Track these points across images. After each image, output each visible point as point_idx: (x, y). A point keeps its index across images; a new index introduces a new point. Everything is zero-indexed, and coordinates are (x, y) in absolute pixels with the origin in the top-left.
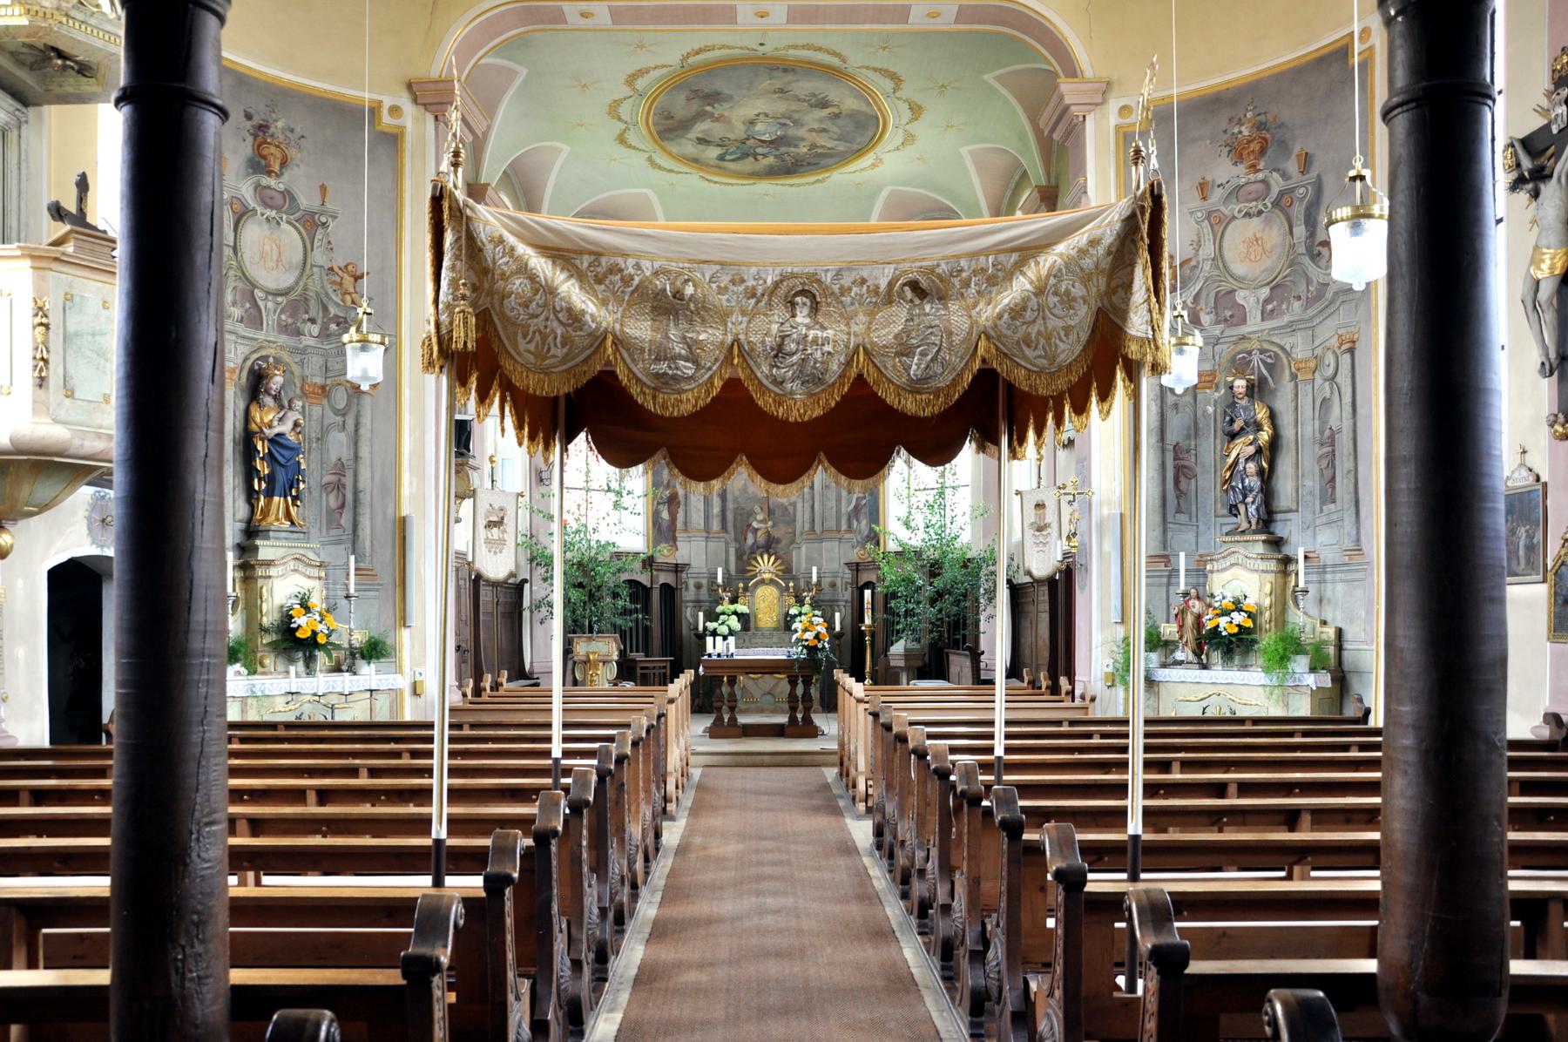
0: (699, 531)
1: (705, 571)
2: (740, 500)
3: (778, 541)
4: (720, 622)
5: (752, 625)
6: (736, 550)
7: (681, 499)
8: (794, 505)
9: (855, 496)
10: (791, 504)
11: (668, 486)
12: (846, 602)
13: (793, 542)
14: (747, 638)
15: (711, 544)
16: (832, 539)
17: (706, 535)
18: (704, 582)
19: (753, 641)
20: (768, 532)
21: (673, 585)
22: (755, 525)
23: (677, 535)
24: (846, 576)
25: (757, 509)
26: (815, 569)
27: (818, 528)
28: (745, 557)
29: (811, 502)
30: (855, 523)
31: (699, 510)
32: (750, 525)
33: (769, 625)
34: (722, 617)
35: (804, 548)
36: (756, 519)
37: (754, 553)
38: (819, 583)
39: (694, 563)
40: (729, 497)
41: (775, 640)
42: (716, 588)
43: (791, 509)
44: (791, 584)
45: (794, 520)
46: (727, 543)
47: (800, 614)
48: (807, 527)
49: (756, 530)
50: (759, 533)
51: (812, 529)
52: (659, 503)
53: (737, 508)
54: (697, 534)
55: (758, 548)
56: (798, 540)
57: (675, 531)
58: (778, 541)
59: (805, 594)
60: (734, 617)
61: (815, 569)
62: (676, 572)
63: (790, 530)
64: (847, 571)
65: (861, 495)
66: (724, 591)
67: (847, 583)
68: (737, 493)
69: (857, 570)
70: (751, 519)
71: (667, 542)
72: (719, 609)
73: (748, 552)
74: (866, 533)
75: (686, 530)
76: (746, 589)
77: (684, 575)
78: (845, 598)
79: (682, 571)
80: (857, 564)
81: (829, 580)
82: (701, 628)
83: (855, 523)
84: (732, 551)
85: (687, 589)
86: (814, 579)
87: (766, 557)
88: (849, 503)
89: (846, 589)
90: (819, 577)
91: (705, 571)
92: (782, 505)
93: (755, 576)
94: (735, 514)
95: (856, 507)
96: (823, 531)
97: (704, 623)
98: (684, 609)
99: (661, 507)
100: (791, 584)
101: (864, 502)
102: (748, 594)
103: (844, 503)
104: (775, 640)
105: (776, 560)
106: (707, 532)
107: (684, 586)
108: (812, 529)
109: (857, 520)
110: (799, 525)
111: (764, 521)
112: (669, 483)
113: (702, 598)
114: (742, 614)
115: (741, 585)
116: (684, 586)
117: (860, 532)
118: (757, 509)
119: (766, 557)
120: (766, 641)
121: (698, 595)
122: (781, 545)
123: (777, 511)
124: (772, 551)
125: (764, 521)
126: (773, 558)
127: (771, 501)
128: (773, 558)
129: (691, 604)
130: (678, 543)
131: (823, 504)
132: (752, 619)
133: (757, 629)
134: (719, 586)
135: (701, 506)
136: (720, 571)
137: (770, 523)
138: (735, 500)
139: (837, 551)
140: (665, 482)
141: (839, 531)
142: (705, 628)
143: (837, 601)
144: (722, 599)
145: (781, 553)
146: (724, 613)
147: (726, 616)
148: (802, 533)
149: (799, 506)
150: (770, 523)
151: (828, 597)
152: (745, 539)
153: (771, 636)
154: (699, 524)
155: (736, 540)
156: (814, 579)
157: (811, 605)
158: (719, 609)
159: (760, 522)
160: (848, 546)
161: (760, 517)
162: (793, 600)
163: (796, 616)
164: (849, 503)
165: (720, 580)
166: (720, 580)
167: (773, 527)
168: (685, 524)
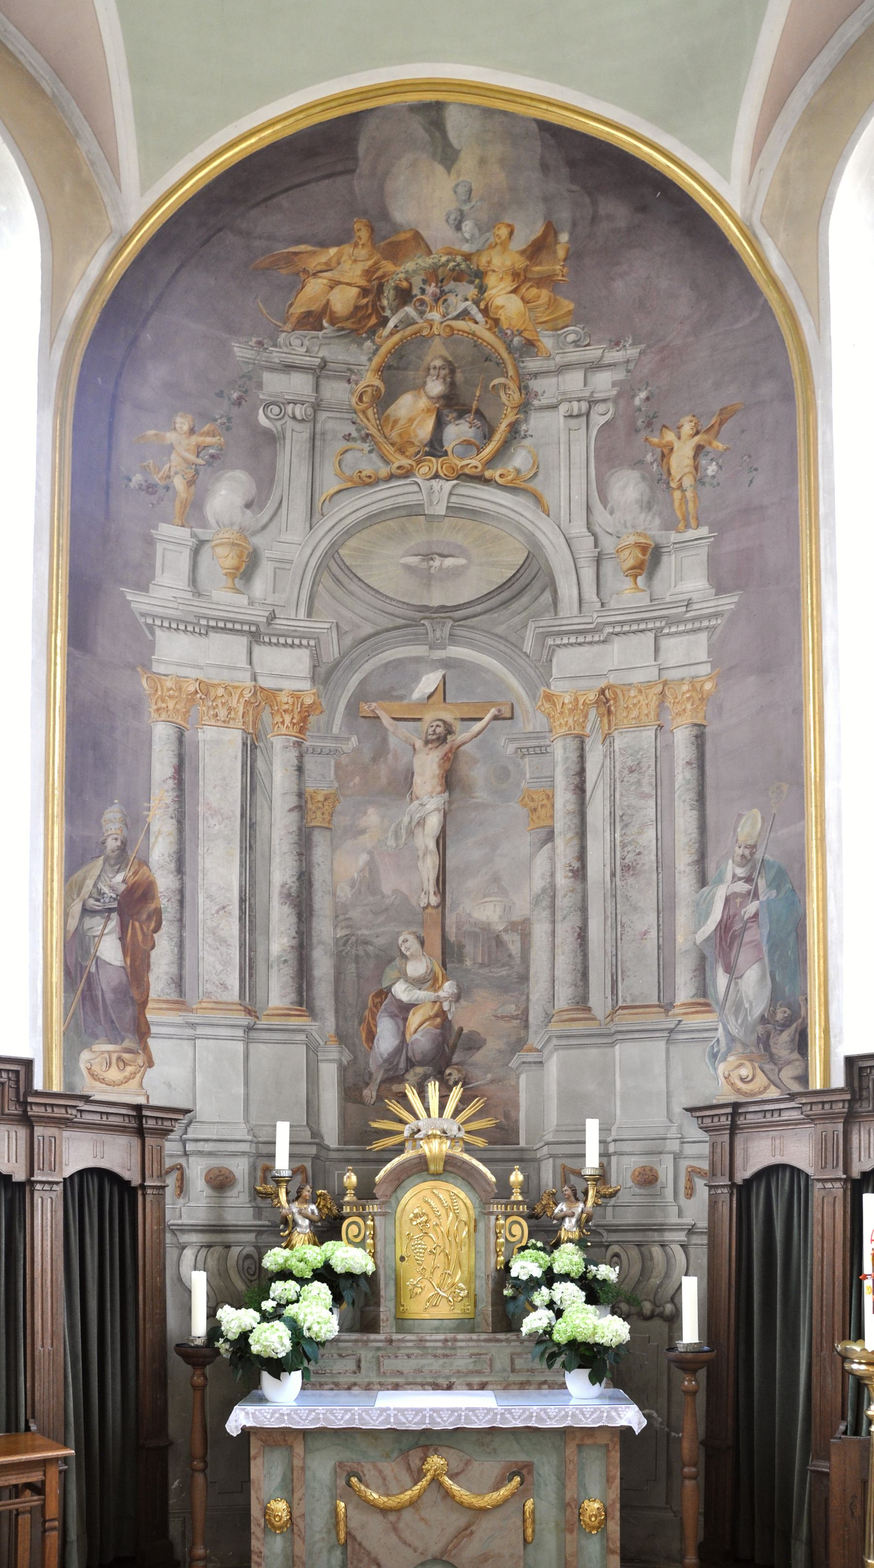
0: (220, 1005)
1: (241, 1132)
2: (355, 914)
3: (474, 1043)
4: (268, 1305)
5: (386, 1310)
6: (343, 1070)
7: (165, 901)
8: (523, 928)
9: (721, 893)
10: (513, 926)
11: (121, 857)
12: (691, 1231)
13: (519, 1044)
14: (366, 1355)
15: (260, 1051)
16: (646, 1033)
17: (245, 1020)
18: (240, 1168)
19: (389, 1364)
20: (442, 1014)
21: (132, 1176)
22: (401, 991)
23: (150, 1016)
24: (689, 1149)
25: (409, 943)
26: (592, 1127)
27: (599, 1000)
28: (370, 1093)
29: (574, 920)
30: (722, 979)
31: (224, 941)
32: (384, 993)
33: (444, 1311)
34: (279, 1289)
35: (553, 1065)
36: (403, 975)
37: (400, 1079)
38: (602, 1177)
39: (204, 1109)
40: (322, 903)
41: (462, 1362)
42: (270, 1187)
43: (513, 943)
44: (517, 1177)
45: (524, 978)
46: (312, 1049)
47: (550, 1278)
48: (564, 996)
49: (404, 1009)
50: (414, 1019)
51: (582, 1002)
52: (86, 911)
53: (346, 939)
54: (217, 1016)
55: (411, 1064)
56: (535, 1040)
57: (143, 1004)
58: (474, 1043)
59: (562, 1207)
60: (321, 1291)
61: (592, 1127)
62: (140, 1132)
63: (511, 1009)
64: (694, 1132)
65: (742, 887)
66: (296, 1197)
67: (693, 1172)
68: (345, 893)
69: (733, 1129)
70: (390, 973)
71: (115, 1037)
72: (274, 1258)
73: (379, 1076)
74: (759, 1009)
75: (180, 1003)
76: (366, 1192)
77: (171, 1146)
78: (688, 1220)
79: (165, 1133)
80: (736, 1106)
81: (632, 1163)
82: (199, 1328)
83: (722, 979)
84: (329, 1074)
85: (182, 1188)
86: (592, 1162)
87: (433, 1090)
88: (701, 915)
89: (690, 1192)
90: (604, 1155)
91: (241, 1132)
92: (486, 928)
93: (399, 1149)
94: (340, 960)
95: (725, 927)
96: (614, 1011)
97: (211, 1314)
98: (171, 1254)
99: (95, 924)
100: (517, 1177)
101: (752, 908)
102: (373, 1208)
103: (683, 917)
104: (462, 1362)
105: (464, 1101)
106: (249, 1012)
107: (171, 1181)
108: (582, 1002)
109: (729, 969)
110: (538, 990)
111: (429, 981)
112: (123, 848)
113: (231, 1218)
114: (350, 1276)
115: (351, 1179)
116: (171, 1181)
117: (738, 1007)
118: (409, 943)
119: (433, 1090)
120: (436, 1365)
121: (218, 1208)
122: (479, 1057)
123: (469, 949)
124: (453, 1073)
125: (429, 981)
126: (456, 1093)
127: (451, 919)
128: (456, 1093)
129: (194, 1238)
130: (152, 1043)
131: (615, 923)
132: (386, 1292)
133: (402, 1323)
134: (278, 1181)
135: (231, 928)
136: (283, 1132)
137: (448, 988)
138: (339, 915)
139: (659, 1068)
140: (112, 844)
141: (666, 1007)
142: (215, 1330)
143: (660, 1229)
144: (288, 1223)
145: (481, 1079)
146: (285, 1275)
147: (292, 1286)
148: (548, 1018)
149: (540, 932)
150: (448, 988)
151: (629, 1218)
152: (371, 1036)
153: (449, 1349)
154: (224, 986)
155: (342, 1038)
156: (592, 1162)
157: (581, 1243)
158: (274, 1258)
159: (418, 983)
160: (698, 1053)
161: (416, 968)
162: (520, 1230)
163: (533, 1284)
164: (701, 914)
165: (282, 1164)
166: (282, 1164)
167: (458, 998)
168: (179, 982)
